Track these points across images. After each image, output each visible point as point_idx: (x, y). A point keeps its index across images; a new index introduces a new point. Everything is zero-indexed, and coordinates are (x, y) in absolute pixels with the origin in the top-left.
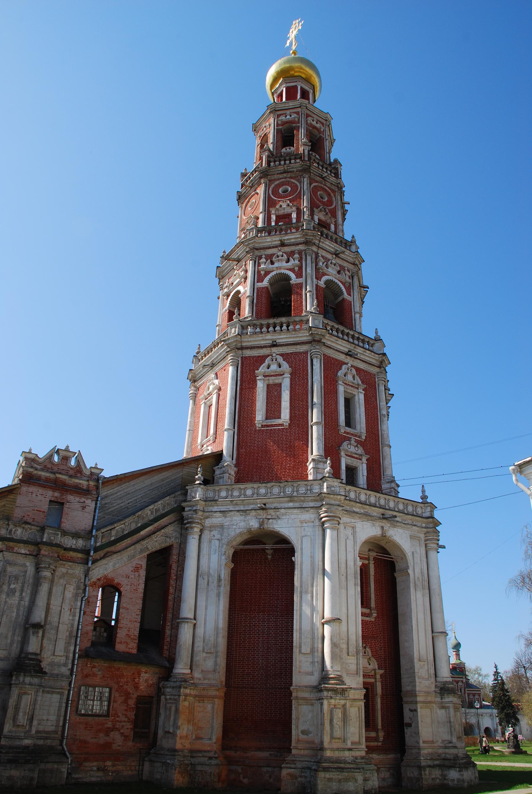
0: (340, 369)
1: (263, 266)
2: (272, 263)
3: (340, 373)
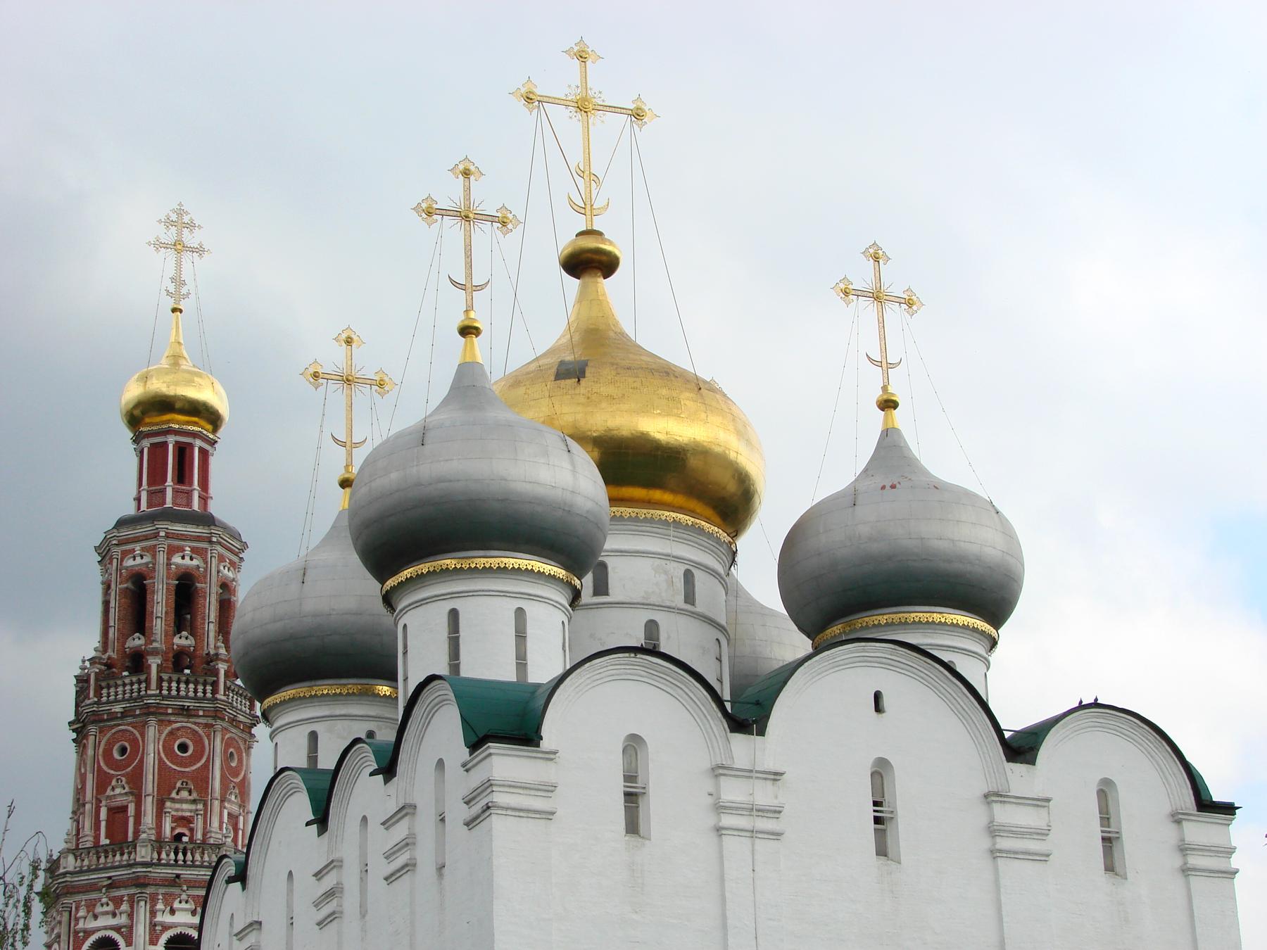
1: (81, 925)
2: (96, 917)
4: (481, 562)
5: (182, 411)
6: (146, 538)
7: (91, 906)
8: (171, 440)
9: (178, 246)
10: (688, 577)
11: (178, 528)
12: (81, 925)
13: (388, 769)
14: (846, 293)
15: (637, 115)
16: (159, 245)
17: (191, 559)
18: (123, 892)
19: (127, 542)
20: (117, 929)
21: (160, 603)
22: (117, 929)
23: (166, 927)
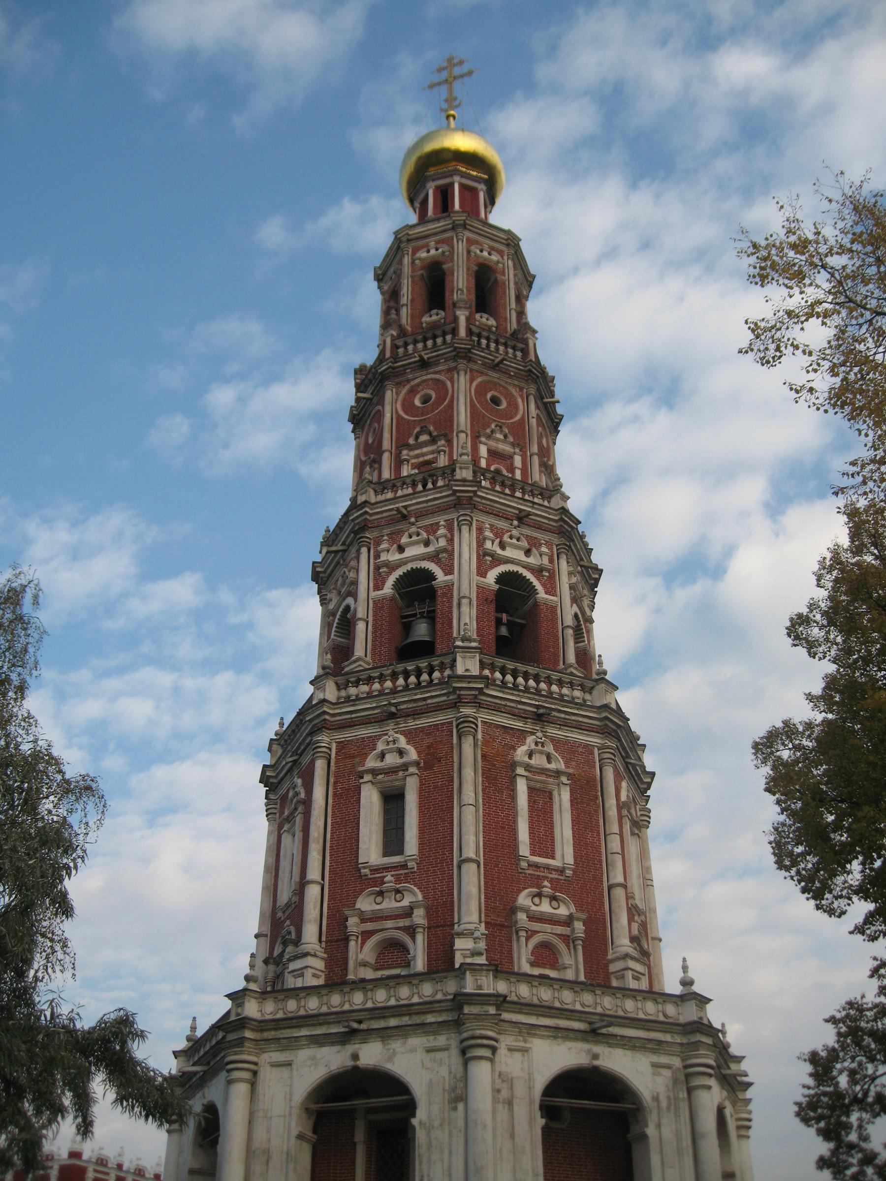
0: (524, 744)
1: (384, 557)
2: (401, 549)
3: (521, 753)
7: (394, 537)
12: (384, 557)
17: (490, 254)
18: (442, 520)
20: (434, 557)
21: (461, 282)
22: (434, 557)
23: (498, 560)
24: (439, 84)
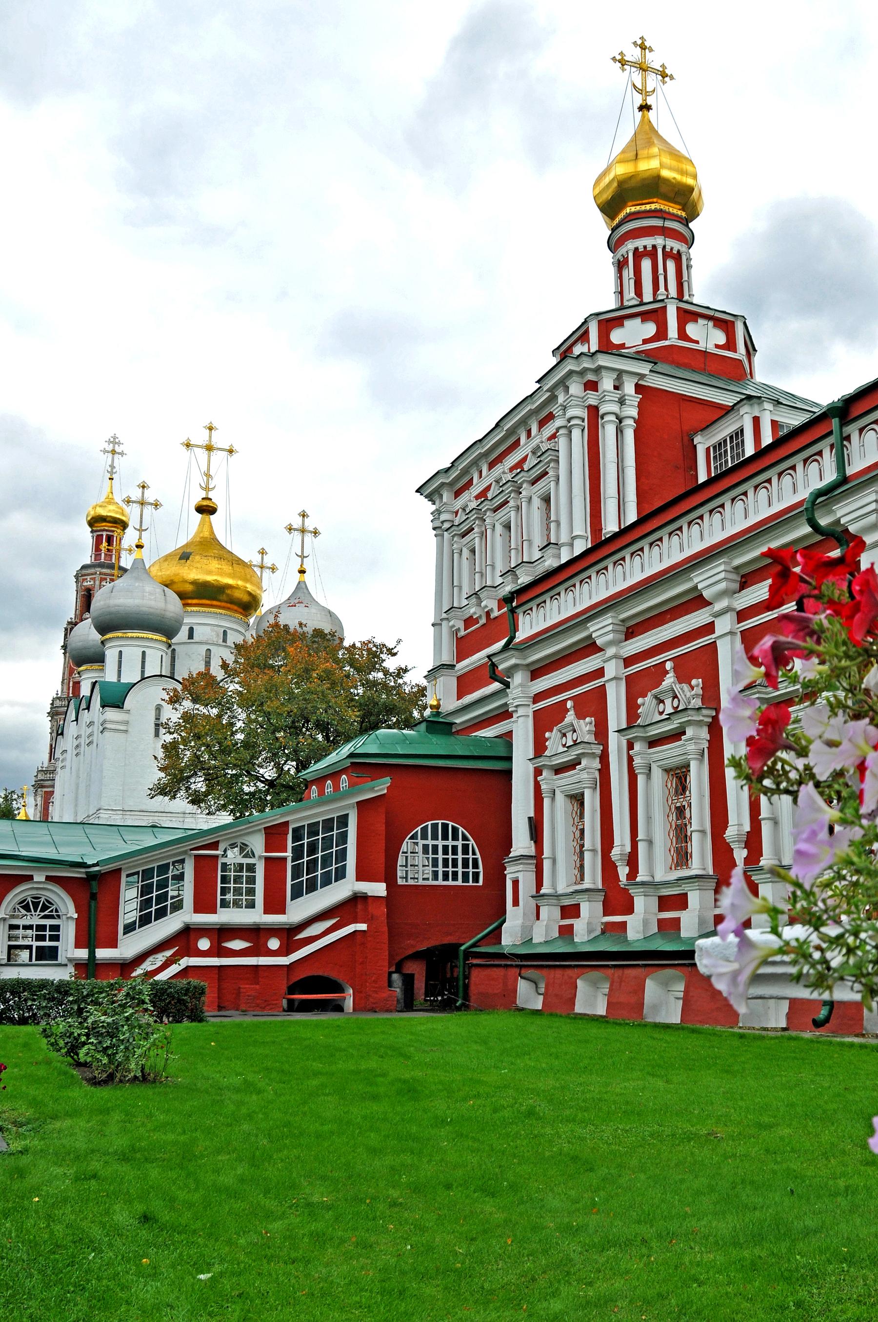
4: (130, 635)
5: (109, 522)
6: (92, 574)
8: (105, 534)
9: (113, 452)
10: (225, 633)
11: (105, 571)
13: (88, 708)
14: (290, 529)
15: (231, 451)
16: (105, 451)
19: (85, 575)
24: (108, 452)
